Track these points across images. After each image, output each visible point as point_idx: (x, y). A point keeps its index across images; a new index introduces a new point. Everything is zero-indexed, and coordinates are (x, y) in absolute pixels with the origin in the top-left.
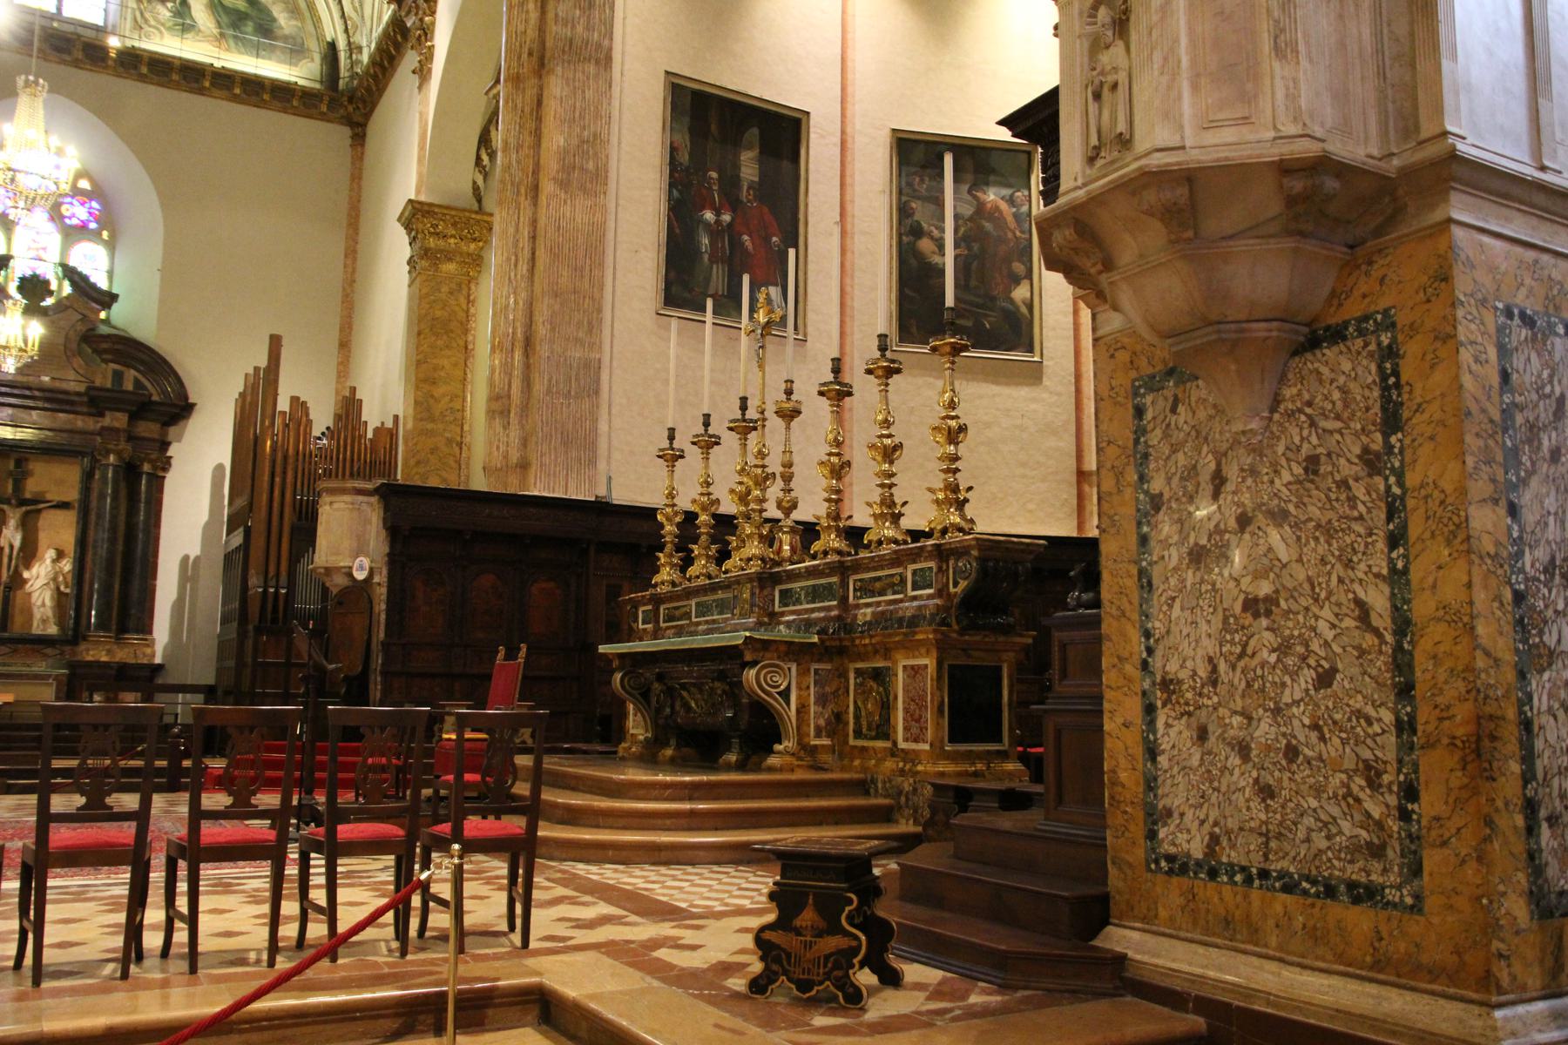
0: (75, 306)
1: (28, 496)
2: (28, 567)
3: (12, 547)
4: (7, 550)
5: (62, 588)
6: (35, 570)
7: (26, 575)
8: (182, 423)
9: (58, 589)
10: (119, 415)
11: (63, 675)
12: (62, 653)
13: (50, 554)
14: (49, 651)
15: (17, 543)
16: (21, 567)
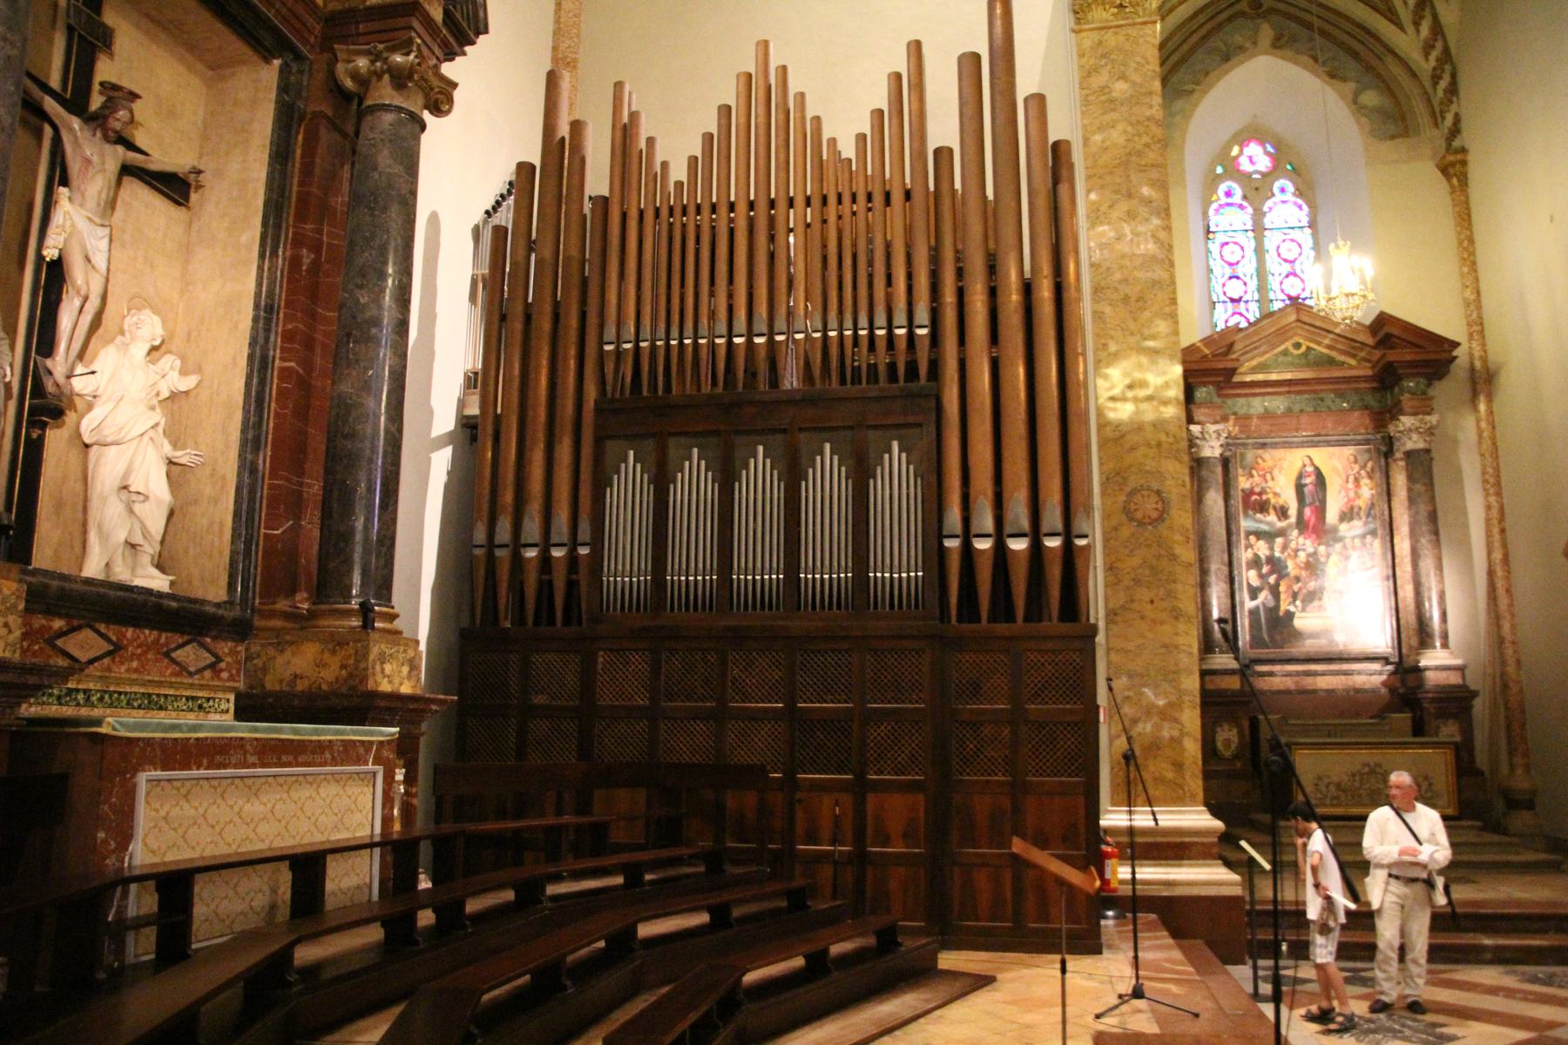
14: (190, 655)
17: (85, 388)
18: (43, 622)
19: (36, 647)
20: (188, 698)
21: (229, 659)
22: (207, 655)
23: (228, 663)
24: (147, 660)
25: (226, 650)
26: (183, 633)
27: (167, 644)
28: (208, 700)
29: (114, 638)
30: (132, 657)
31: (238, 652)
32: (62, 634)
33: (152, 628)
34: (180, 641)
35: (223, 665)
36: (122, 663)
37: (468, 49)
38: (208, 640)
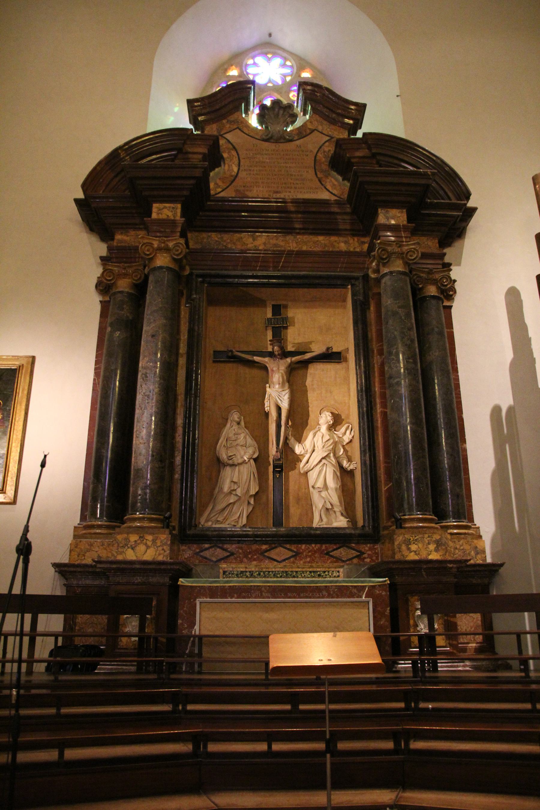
0: (320, 128)
1: (290, 348)
2: (300, 440)
3: (279, 409)
4: (274, 414)
5: (345, 464)
6: (308, 443)
7: (298, 449)
8: (457, 244)
9: (341, 467)
10: (394, 212)
11: (382, 586)
12: (360, 556)
13: (326, 418)
14: (342, 553)
15: (285, 405)
16: (292, 440)
17: (301, 453)
18: (257, 547)
19: (255, 557)
20: (310, 572)
21: (370, 552)
22: (354, 552)
23: (369, 554)
24: (315, 557)
25: (367, 548)
26: (335, 544)
27: (327, 549)
28: (324, 572)
29: (295, 550)
30: (306, 556)
31: (376, 549)
32: (267, 551)
33: (316, 543)
34: (335, 547)
35: (366, 555)
36: (301, 560)
37: (471, 204)
38: (354, 545)
